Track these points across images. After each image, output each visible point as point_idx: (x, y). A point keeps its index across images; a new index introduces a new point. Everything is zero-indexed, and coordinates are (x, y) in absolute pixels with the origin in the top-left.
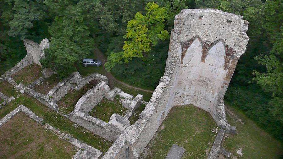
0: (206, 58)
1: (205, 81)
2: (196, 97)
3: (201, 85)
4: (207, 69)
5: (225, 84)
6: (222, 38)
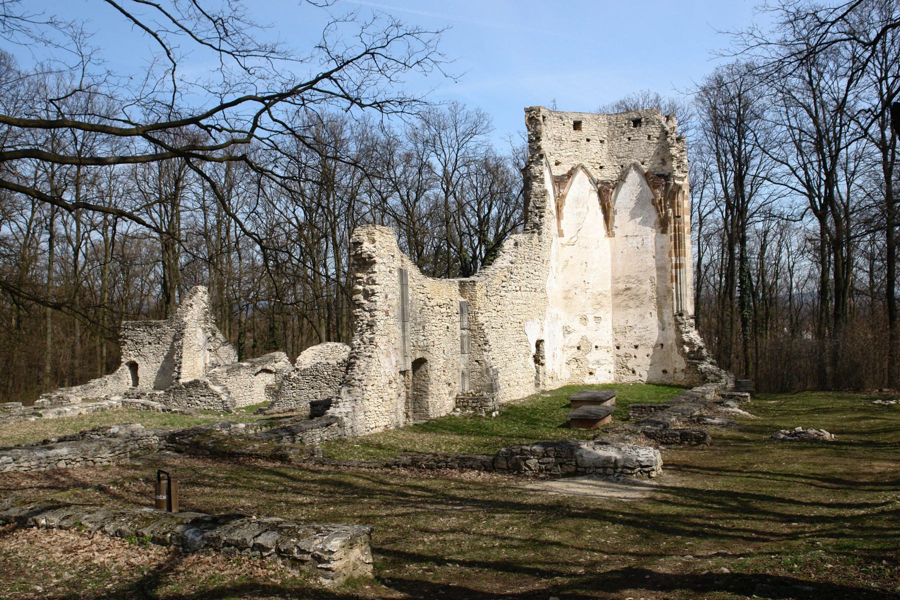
0: (616, 224)
1: (629, 289)
2: (621, 352)
3: (624, 304)
5: (636, 111)
6: (633, 161)
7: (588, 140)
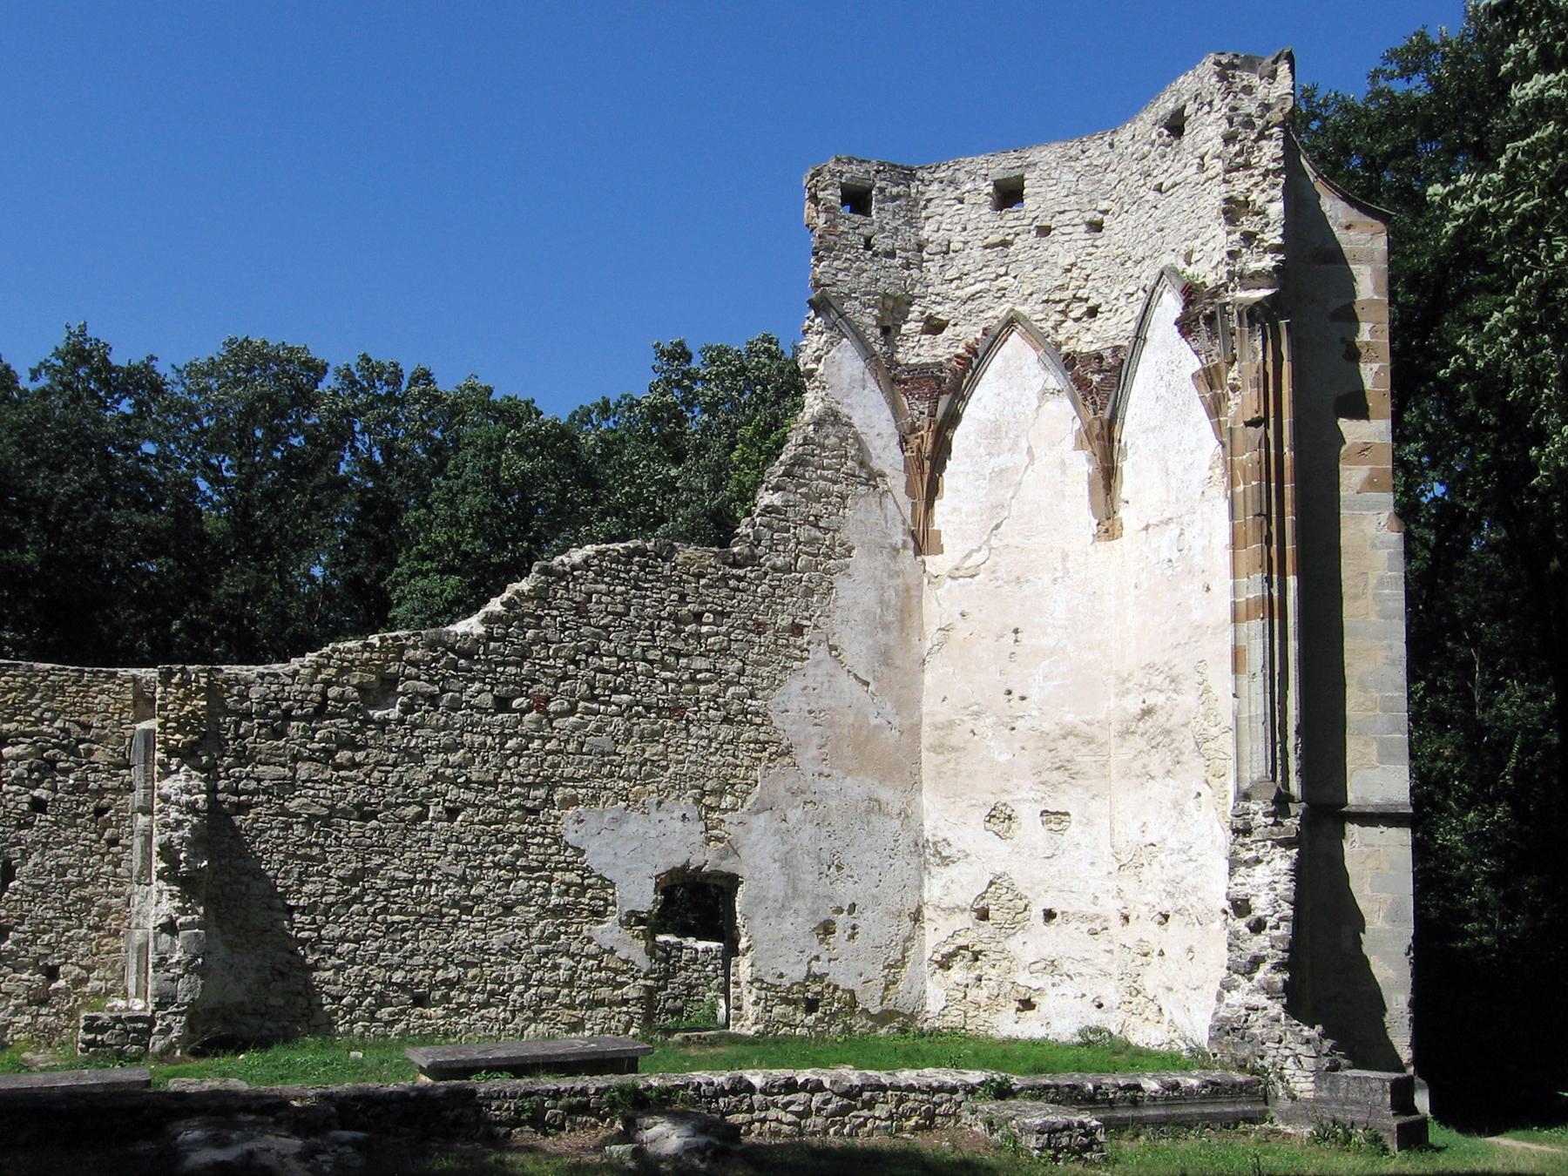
3: (1137, 766)
4: (1144, 576)
7: (1044, 231)
